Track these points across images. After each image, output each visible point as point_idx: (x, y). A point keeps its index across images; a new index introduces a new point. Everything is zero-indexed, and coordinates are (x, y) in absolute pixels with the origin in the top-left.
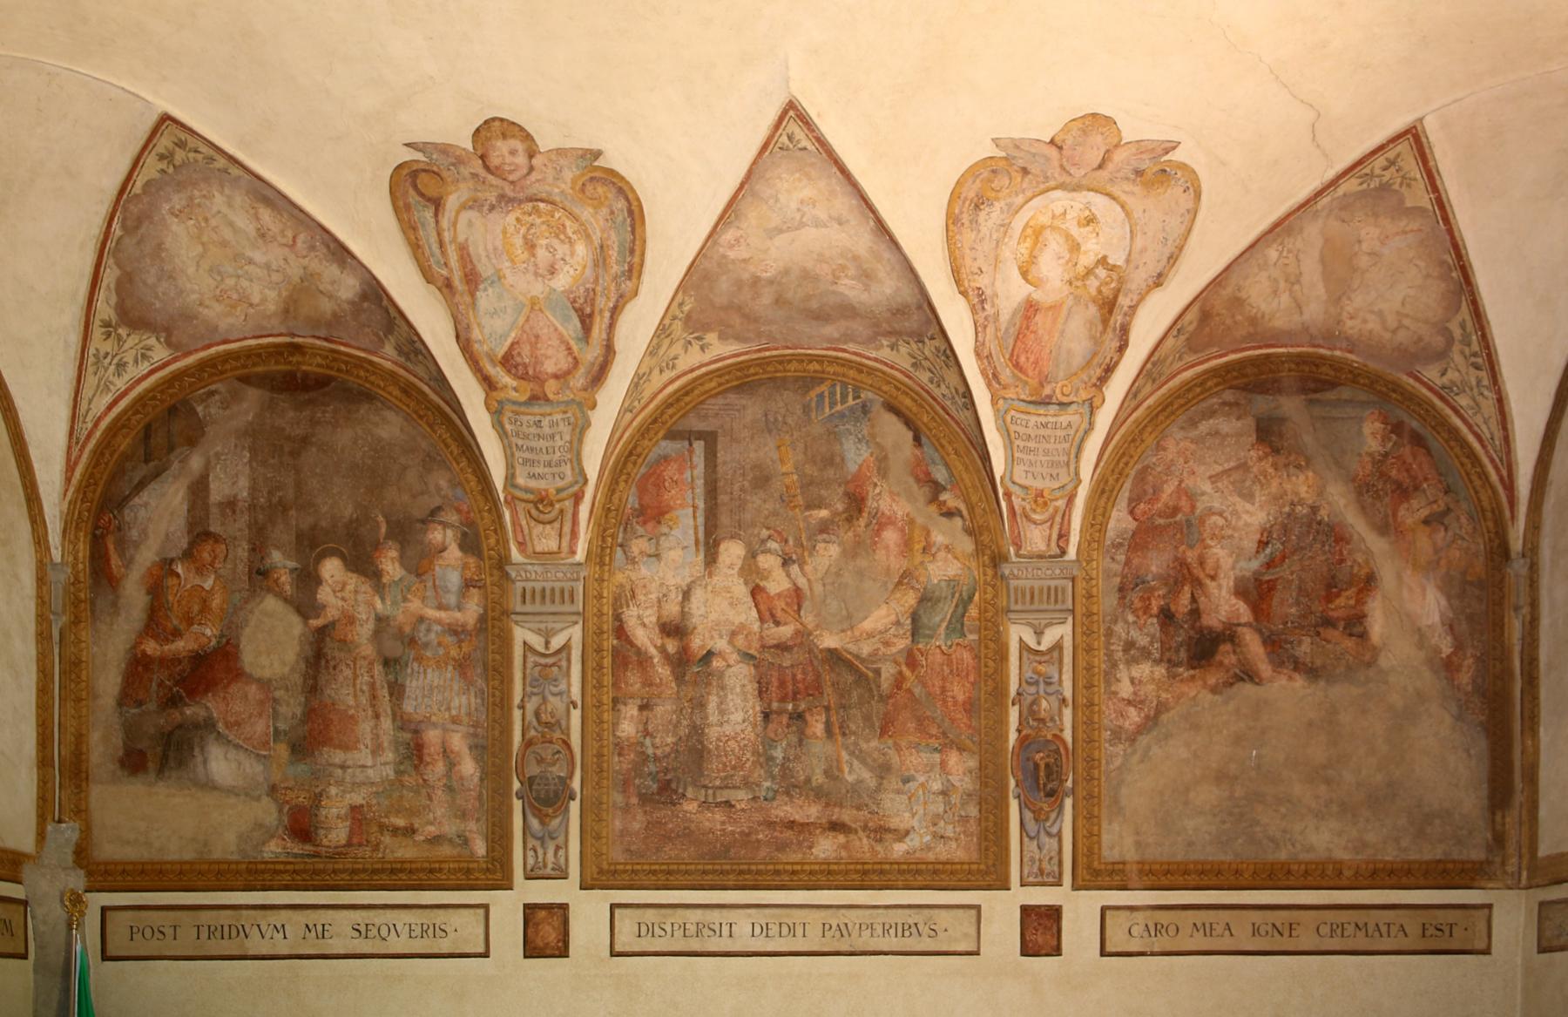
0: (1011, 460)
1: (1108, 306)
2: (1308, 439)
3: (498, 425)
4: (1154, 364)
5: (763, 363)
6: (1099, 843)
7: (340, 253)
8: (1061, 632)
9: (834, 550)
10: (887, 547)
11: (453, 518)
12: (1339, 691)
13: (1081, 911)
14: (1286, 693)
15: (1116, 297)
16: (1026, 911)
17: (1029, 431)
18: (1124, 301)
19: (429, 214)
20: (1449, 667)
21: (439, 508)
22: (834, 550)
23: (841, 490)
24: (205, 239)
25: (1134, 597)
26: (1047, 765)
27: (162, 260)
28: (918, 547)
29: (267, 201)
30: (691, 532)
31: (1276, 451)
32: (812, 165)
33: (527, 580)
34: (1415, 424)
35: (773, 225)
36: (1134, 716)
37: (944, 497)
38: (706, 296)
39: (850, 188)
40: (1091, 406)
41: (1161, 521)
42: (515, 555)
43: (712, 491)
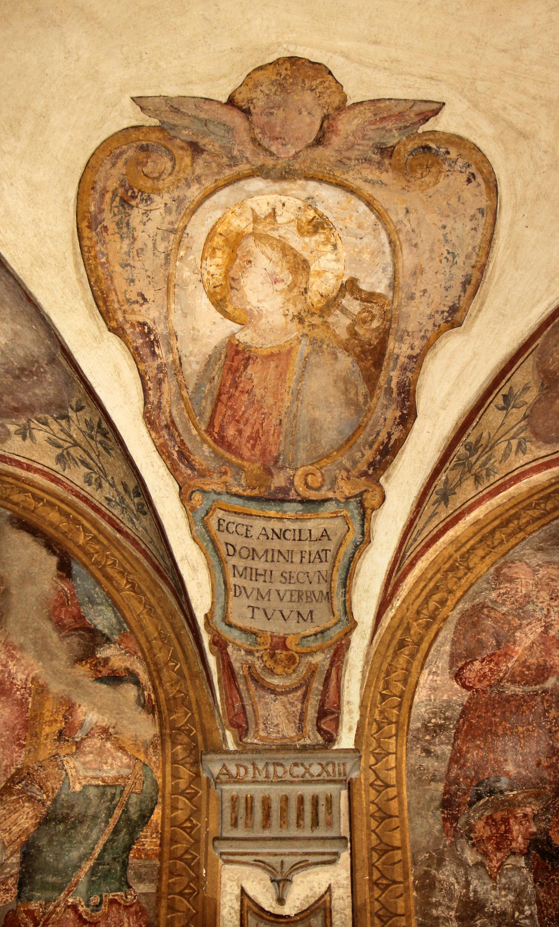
0: (223, 589)
37: (105, 652)
40: (361, 505)
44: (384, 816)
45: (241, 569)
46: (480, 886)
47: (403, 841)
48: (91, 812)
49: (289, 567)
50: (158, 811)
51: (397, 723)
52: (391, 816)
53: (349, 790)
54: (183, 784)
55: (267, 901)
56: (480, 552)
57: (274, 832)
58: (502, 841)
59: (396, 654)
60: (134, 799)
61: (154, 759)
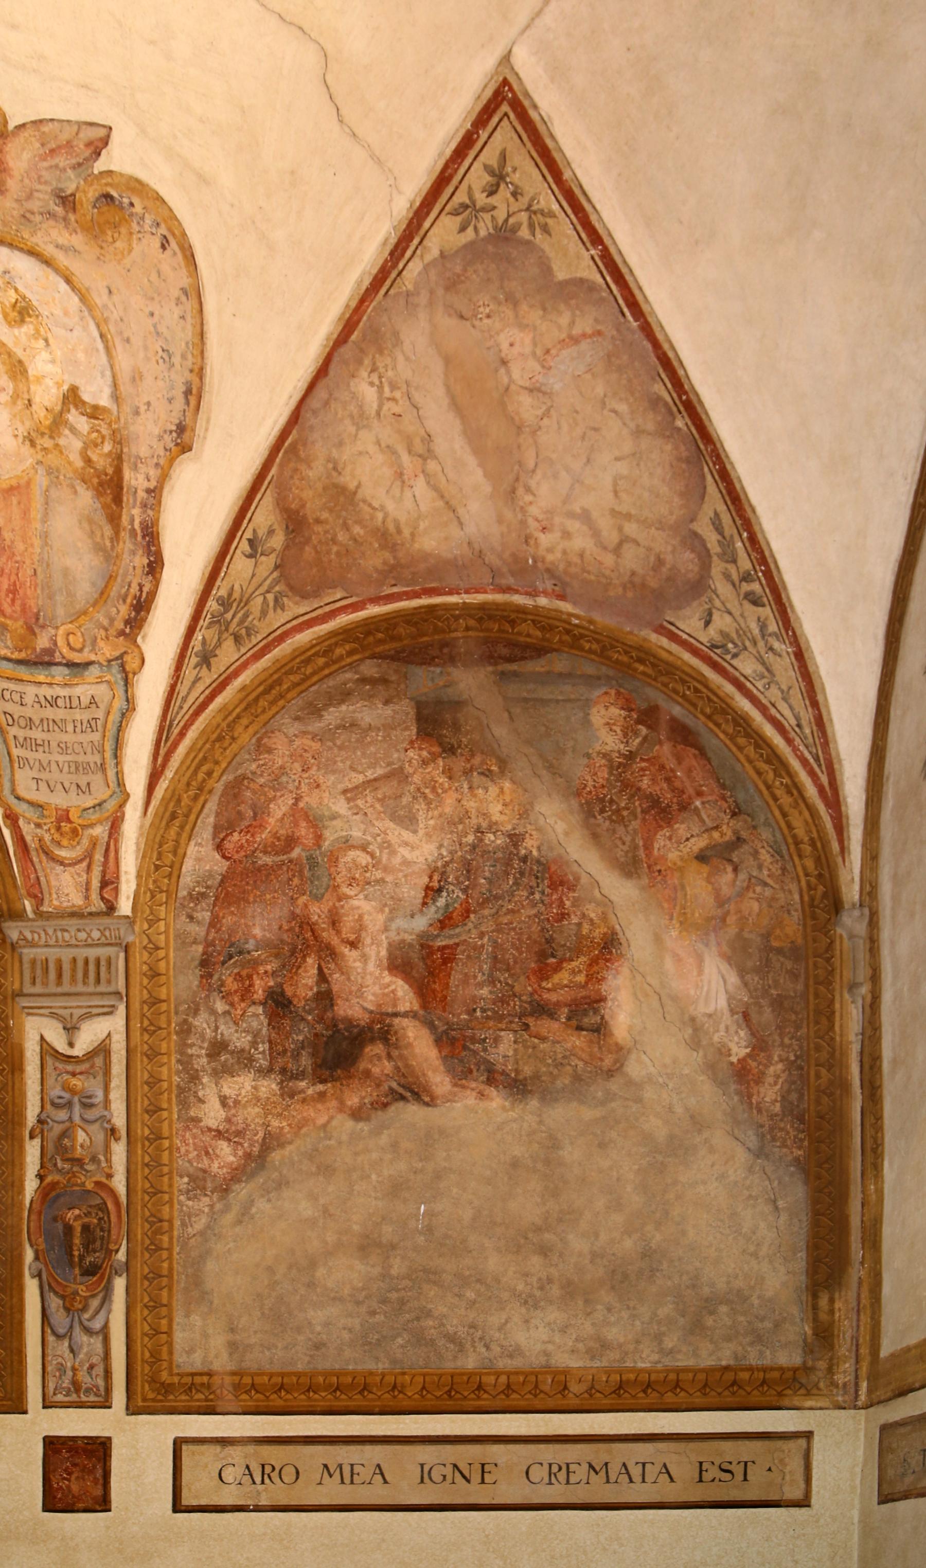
1: (111, 488)
2: (500, 731)
4: (226, 603)
6: (170, 1344)
8: (106, 1028)
12: (561, 1114)
13: (141, 1446)
14: (476, 1120)
15: (118, 471)
16: (52, 1445)
17: (28, 712)
18: (136, 480)
20: (744, 1075)
25: (227, 976)
26: (86, 1228)
31: (450, 750)
34: (677, 711)
36: (226, 1153)
41: (268, 860)
44: (154, 974)
45: (21, 740)
46: (226, 1030)
47: (168, 995)
51: (167, 891)
52: (159, 975)
53: (126, 952)
55: (60, 1045)
56: (244, 721)
58: (246, 993)
59: (168, 826)
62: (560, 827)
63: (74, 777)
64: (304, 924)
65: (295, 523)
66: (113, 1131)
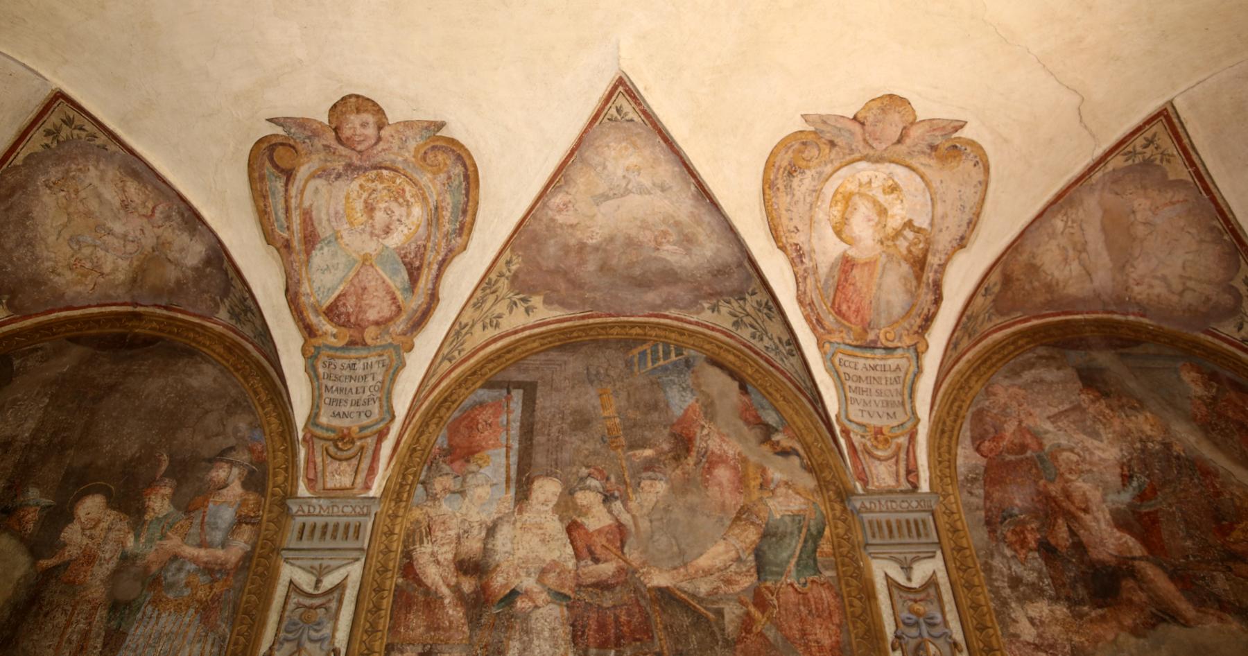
0: (844, 400)
3: (311, 370)
4: (969, 318)
5: (586, 329)
7: (192, 219)
9: (661, 487)
10: (720, 484)
11: (244, 457)
17: (859, 373)
19: (280, 185)
21: (232, 448)
22: (661, 487)
23: (666, 432)
24: (71, 210)
27: (26, 228)
28: (754, 484)
29: (135, 175)
30: (503, 470)
32: (638, 134)
33: (310, 514)
34: (1229, 374)
35: (600, 191)
38: (534, 254)
39: (672, 156)
40: (916, 350)
42: (303, 490)
43: (528, 431)
44: (956, 531)
48: (789, 530)
49: (880, 387)
50: (827, 529)
53: (933, 515)
54: (838, 513)
55: (901, 579)
57: (897, 540)
60: (812, 523)
61: (819, 500)
62: (1192, 439)
63: (885, 409)
64: (1048, 497)
65: (1007, 280)
66: (955, 645)
